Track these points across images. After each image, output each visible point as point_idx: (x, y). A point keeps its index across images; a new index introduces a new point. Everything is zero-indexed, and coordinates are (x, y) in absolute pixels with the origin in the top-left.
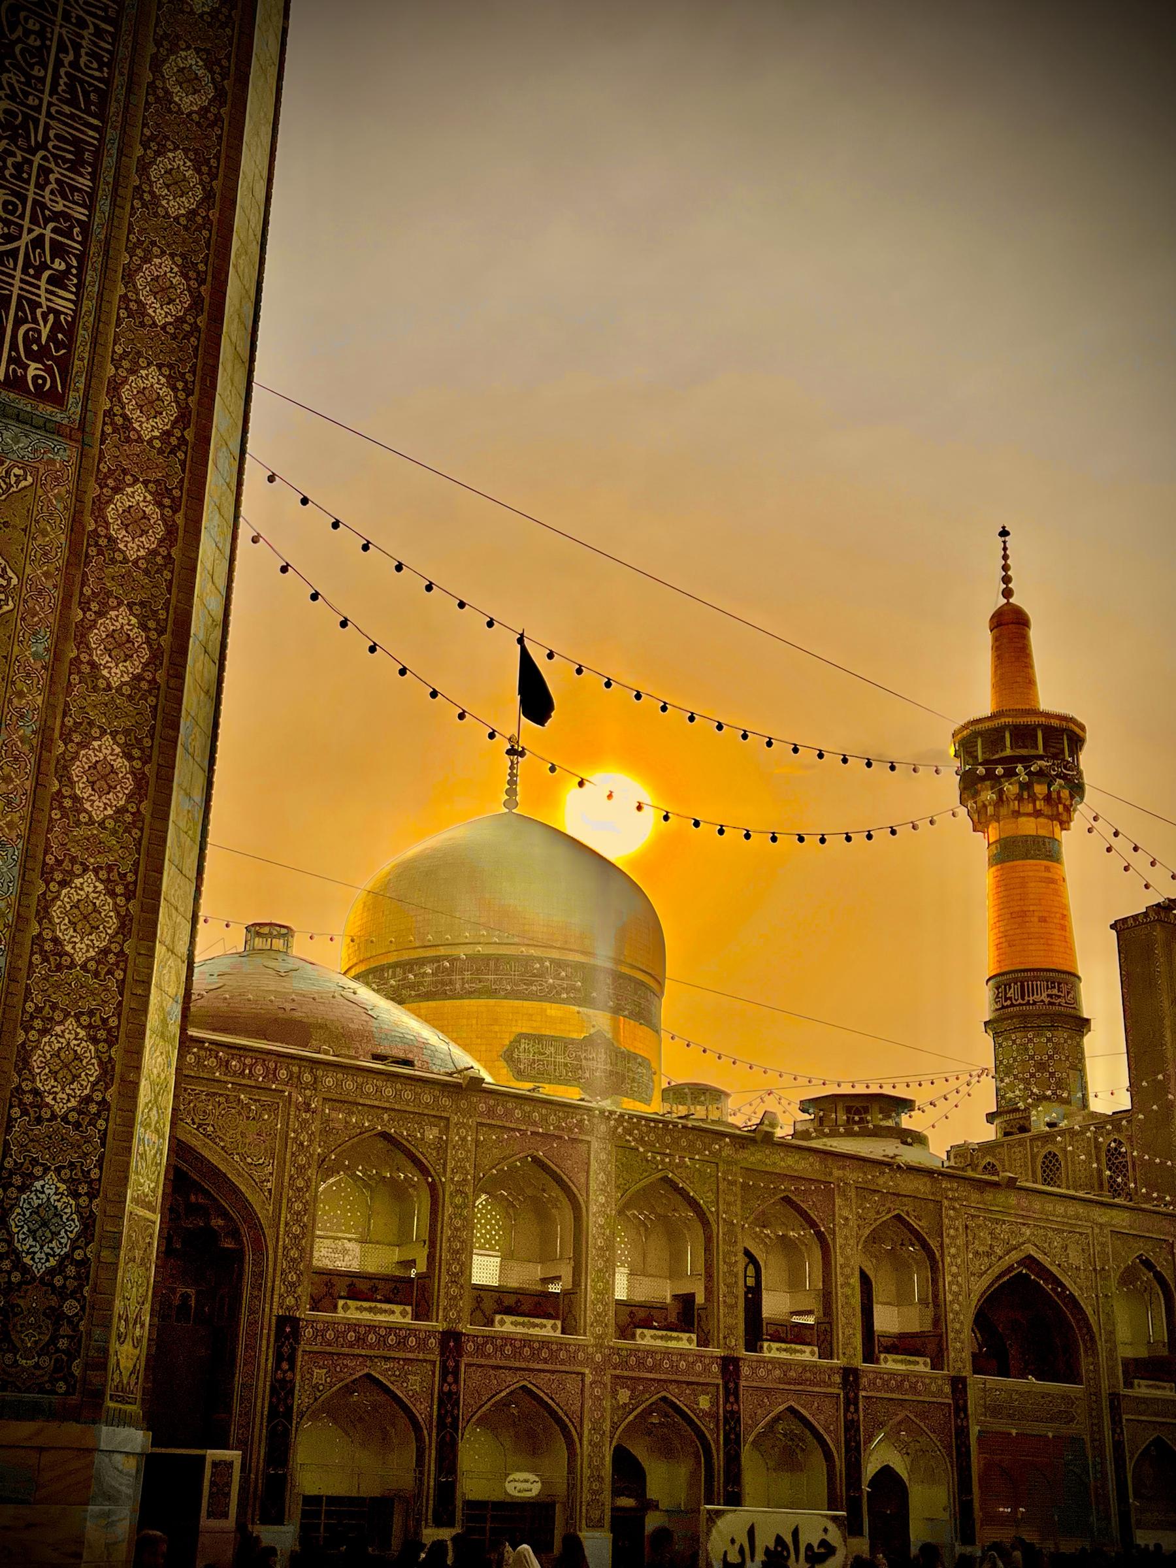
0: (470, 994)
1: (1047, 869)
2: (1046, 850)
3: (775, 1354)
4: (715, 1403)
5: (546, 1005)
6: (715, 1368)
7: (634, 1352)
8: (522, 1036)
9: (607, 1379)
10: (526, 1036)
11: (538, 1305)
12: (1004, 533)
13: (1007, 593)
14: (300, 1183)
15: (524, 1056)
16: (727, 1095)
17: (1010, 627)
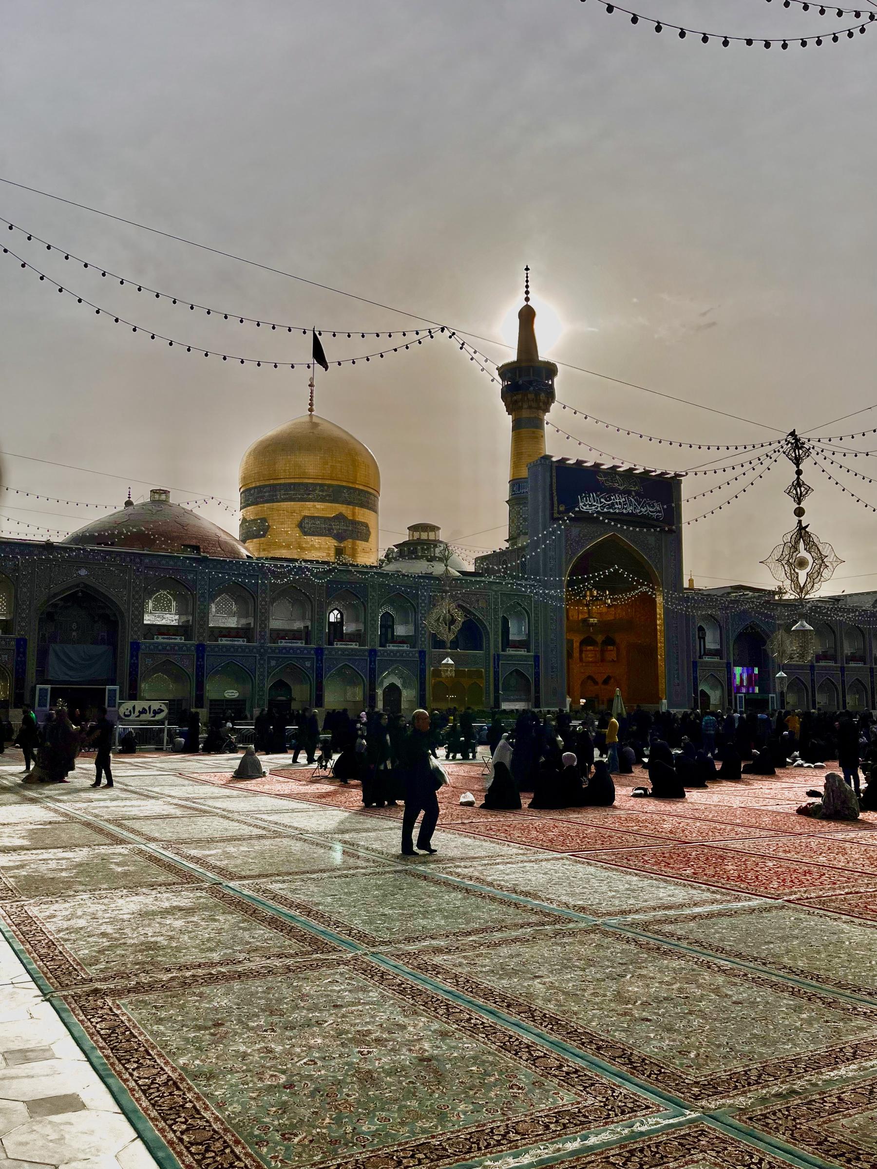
0: (284, 500)
1: (534, 432)
2: (538, 424)
3: (339, 646)
4: (312, 664)
5: (316, 503)
6: (312, 652)
7: (278, 648)
8: (305, 517)
9: (266, 658)
10: (308, 517)
11: (238, 632)
12: (527, 269)
13: (527, 299)
14: (137, 597)
15: (307, 525)
16: (439, 528)
17: (527, 316)
